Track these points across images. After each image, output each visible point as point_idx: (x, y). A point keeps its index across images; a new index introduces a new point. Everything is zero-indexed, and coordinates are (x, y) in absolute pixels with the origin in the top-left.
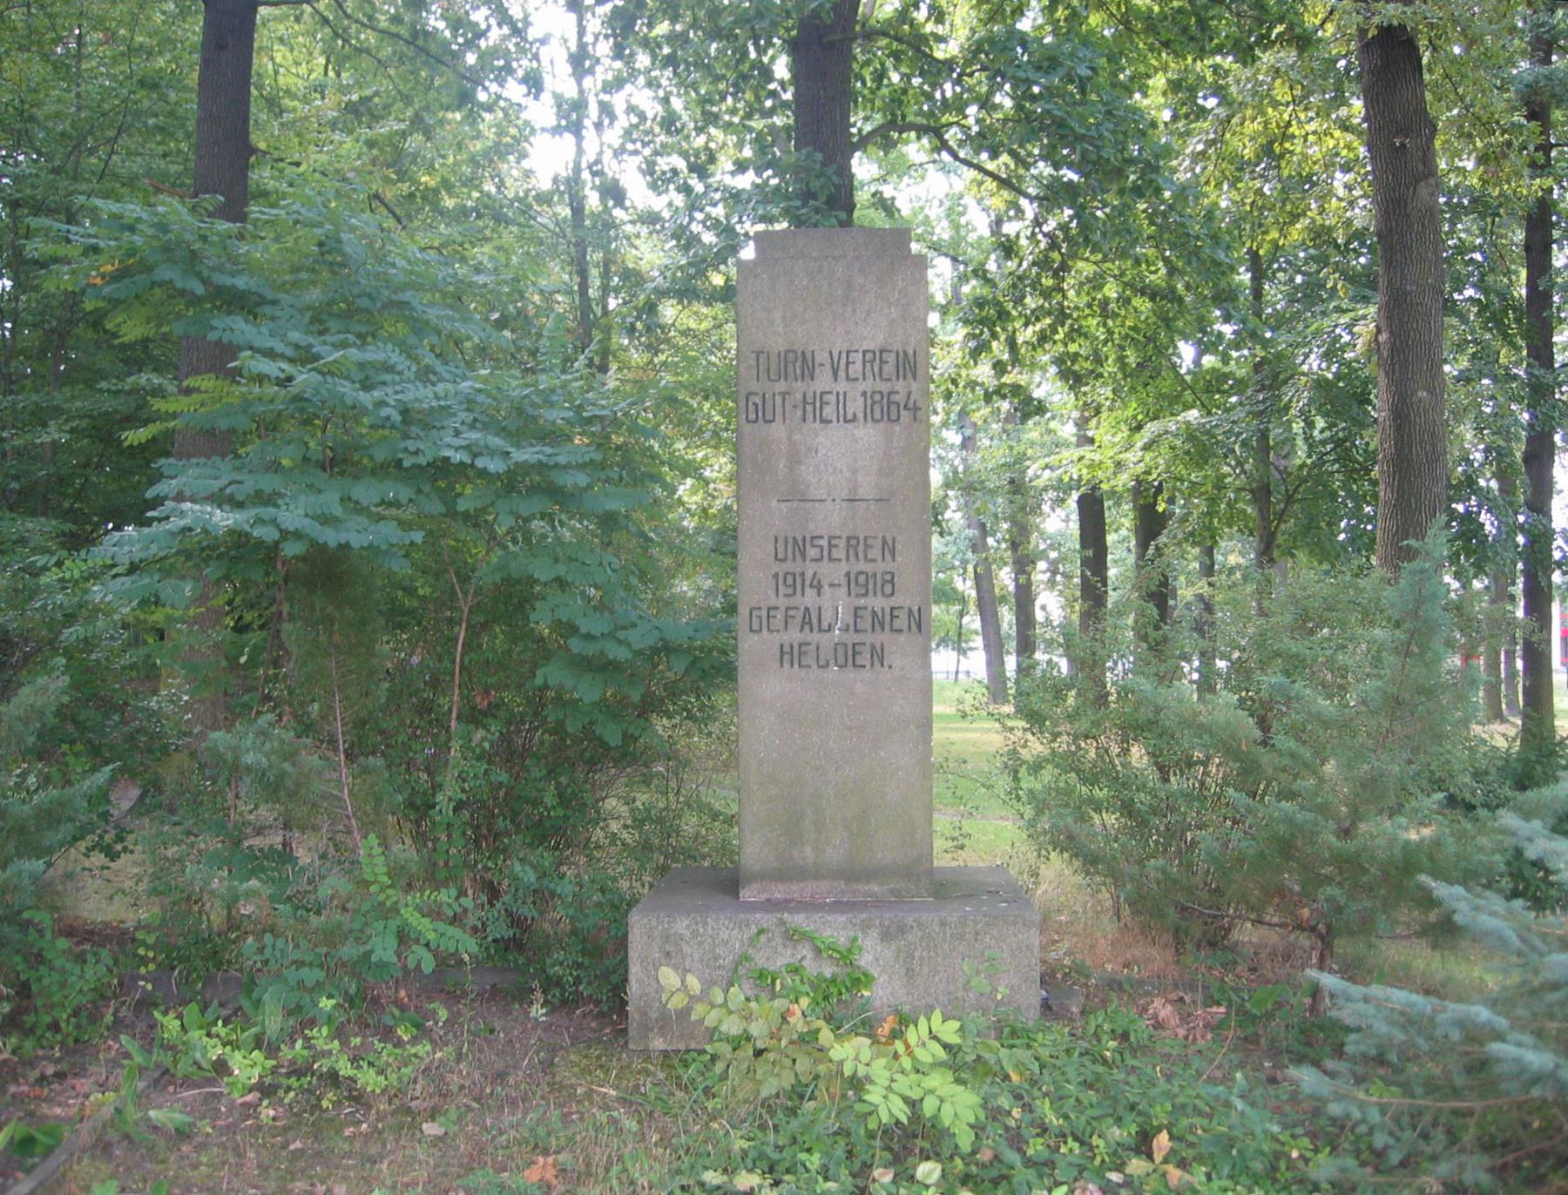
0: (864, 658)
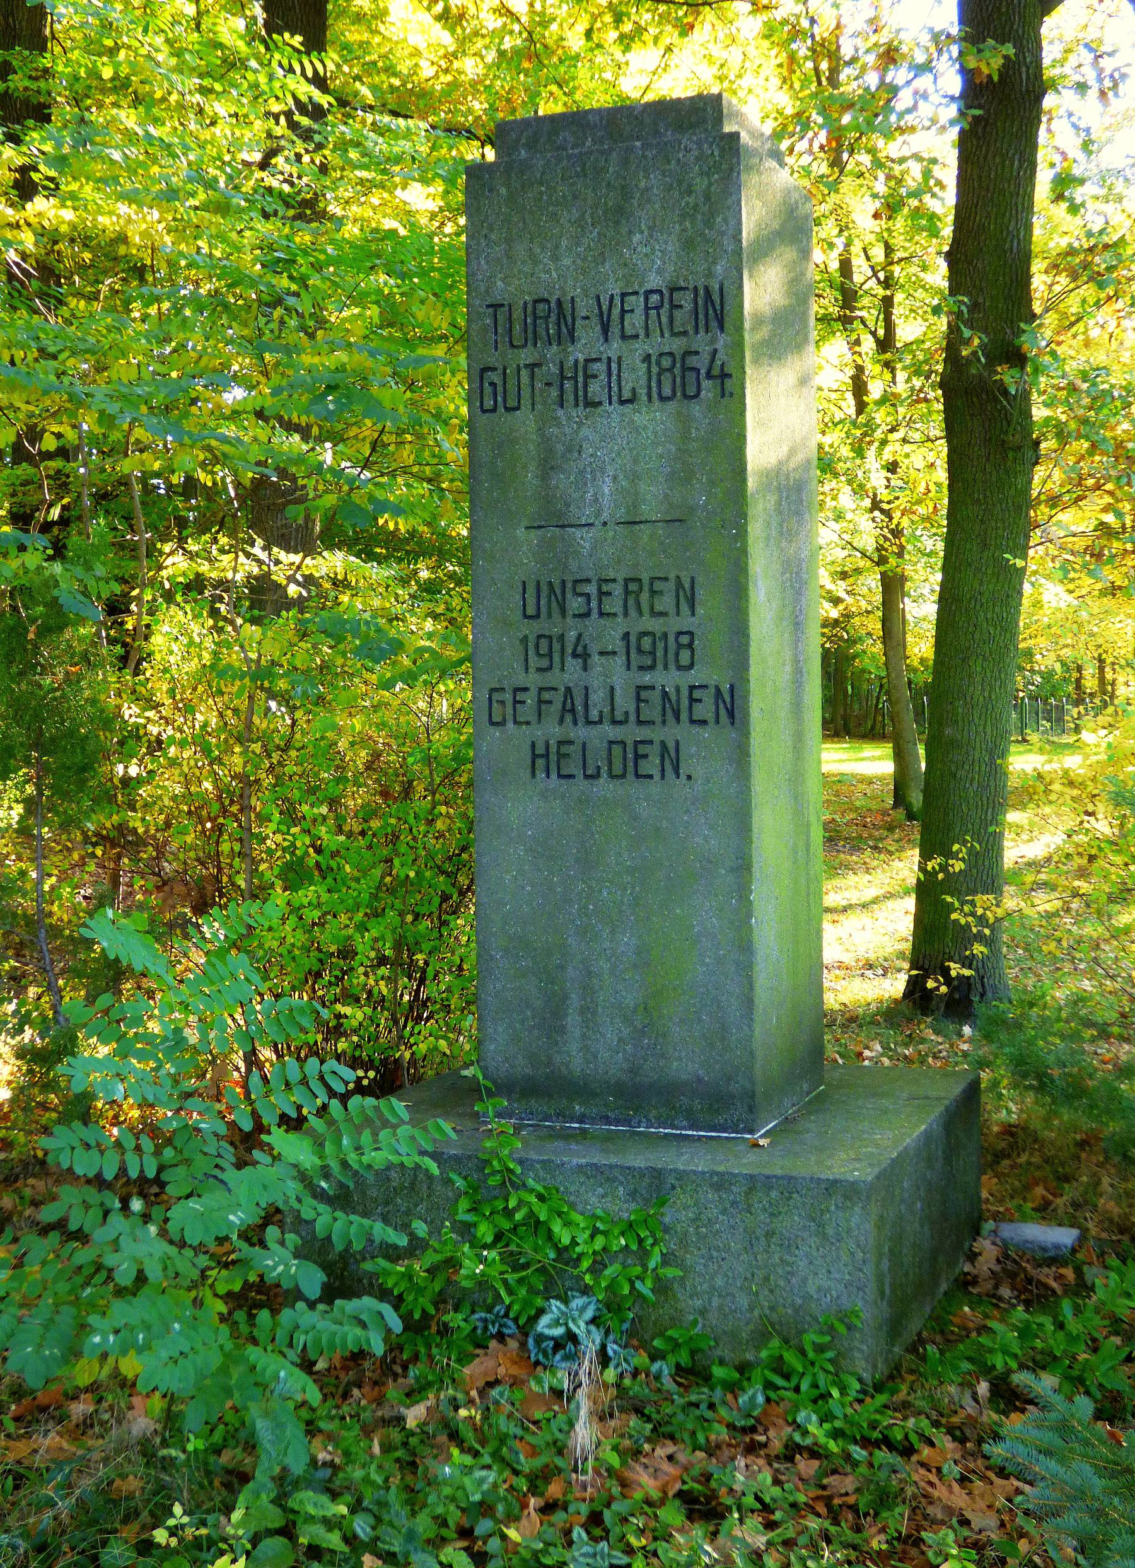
0: (651, 766)
